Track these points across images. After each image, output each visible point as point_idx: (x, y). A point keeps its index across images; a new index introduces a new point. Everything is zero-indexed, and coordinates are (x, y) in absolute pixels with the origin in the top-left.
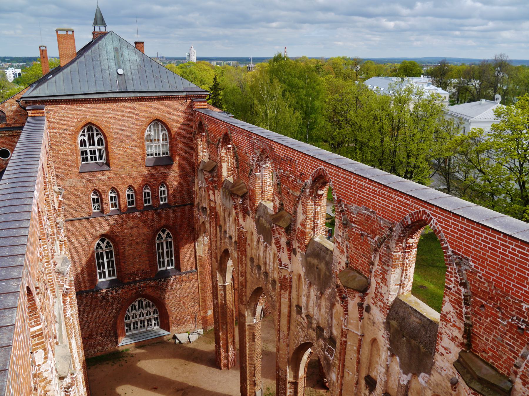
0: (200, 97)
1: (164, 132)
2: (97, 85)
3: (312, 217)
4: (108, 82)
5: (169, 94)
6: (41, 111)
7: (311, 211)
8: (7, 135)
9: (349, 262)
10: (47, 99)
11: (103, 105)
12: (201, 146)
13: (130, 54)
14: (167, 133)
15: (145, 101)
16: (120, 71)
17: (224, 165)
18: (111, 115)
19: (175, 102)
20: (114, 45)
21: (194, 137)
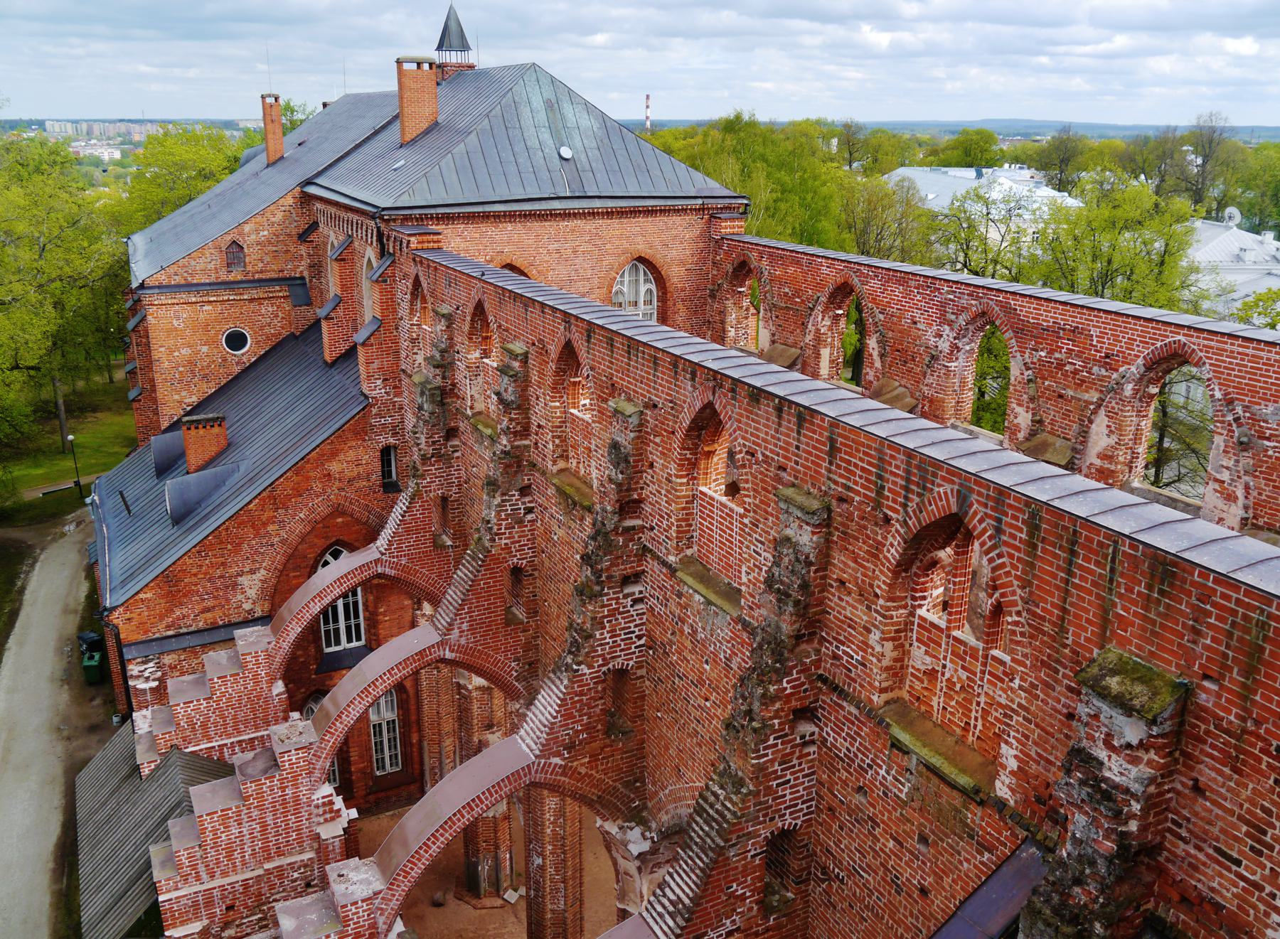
0: (728, 208)
1: (649, 286)
2: (525, 182)
3: (1131, 440)
4: (545, 175)
5: (670, 202)
6: (435, 238)
7: (1129, 428)
8: (246, 297)
9: (1251, 515)
10: (432, 211)
11: (536, 225)
12: (734, 316)
13: (577, 114)
14: (653, 287)
15: (620, 218)
16: (566, 152)
17: (825, 353)
18: (551, 247)
19: (676, 220)
20: (544, 95)
21: (713, 296)
